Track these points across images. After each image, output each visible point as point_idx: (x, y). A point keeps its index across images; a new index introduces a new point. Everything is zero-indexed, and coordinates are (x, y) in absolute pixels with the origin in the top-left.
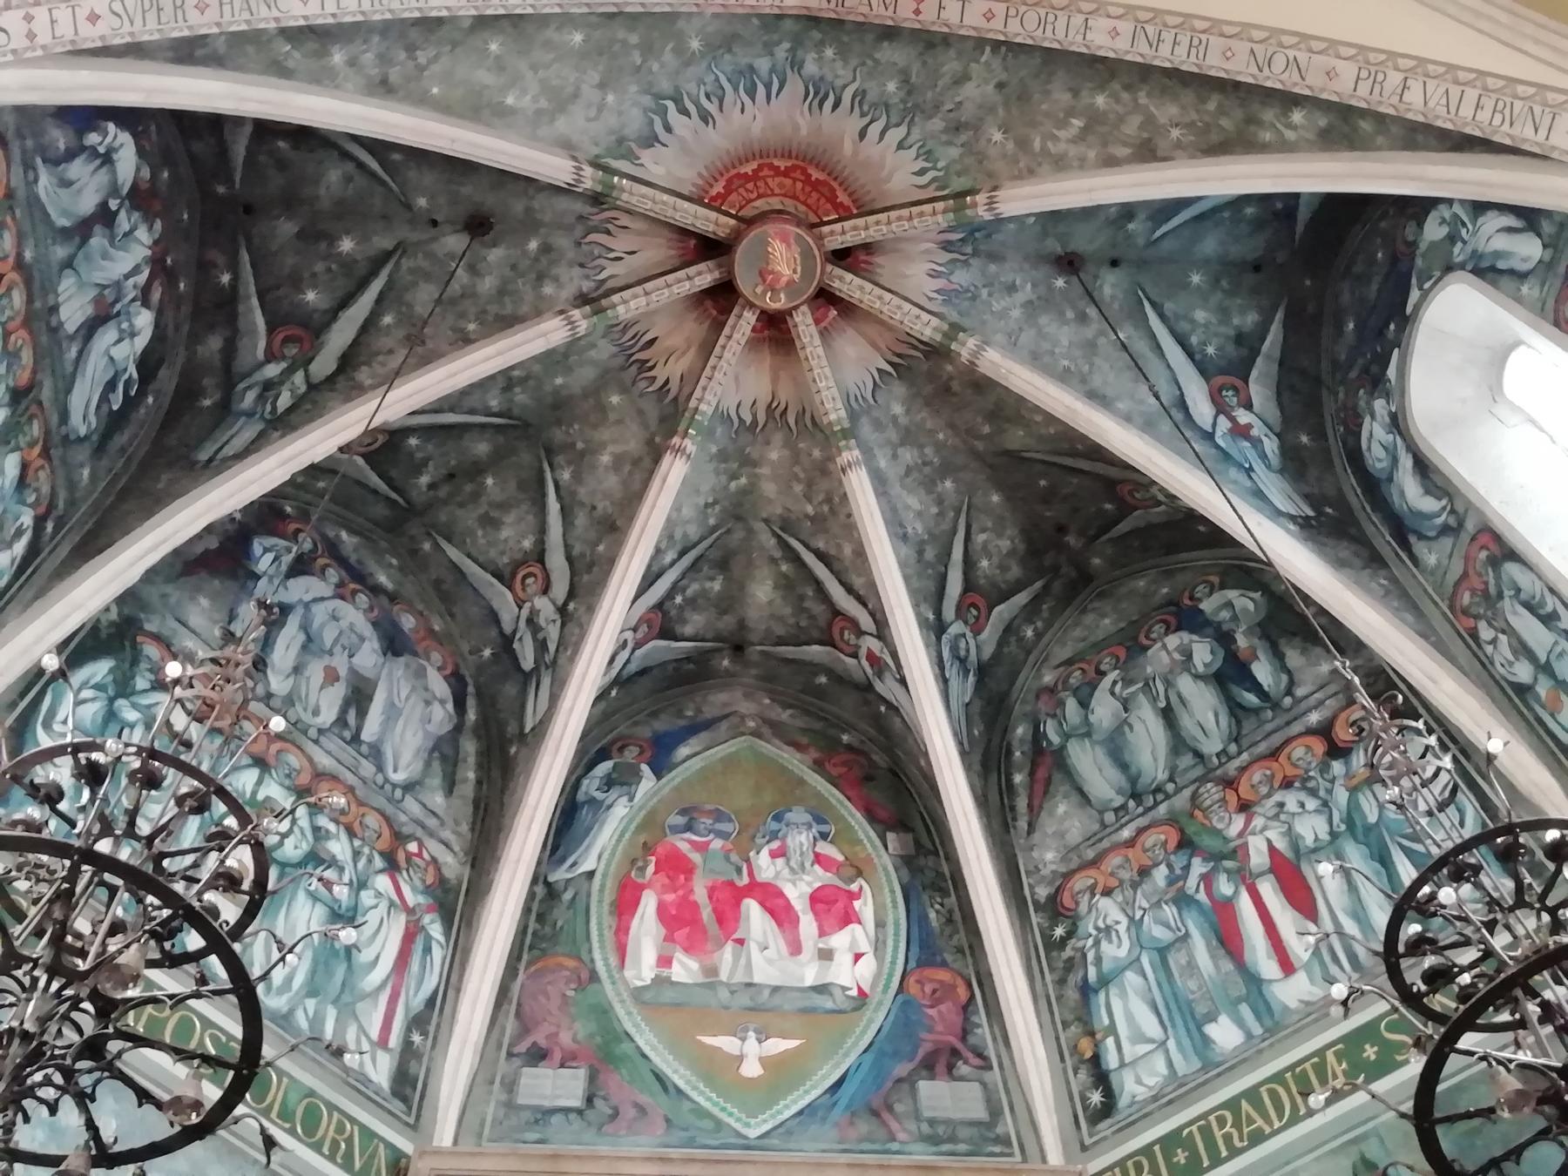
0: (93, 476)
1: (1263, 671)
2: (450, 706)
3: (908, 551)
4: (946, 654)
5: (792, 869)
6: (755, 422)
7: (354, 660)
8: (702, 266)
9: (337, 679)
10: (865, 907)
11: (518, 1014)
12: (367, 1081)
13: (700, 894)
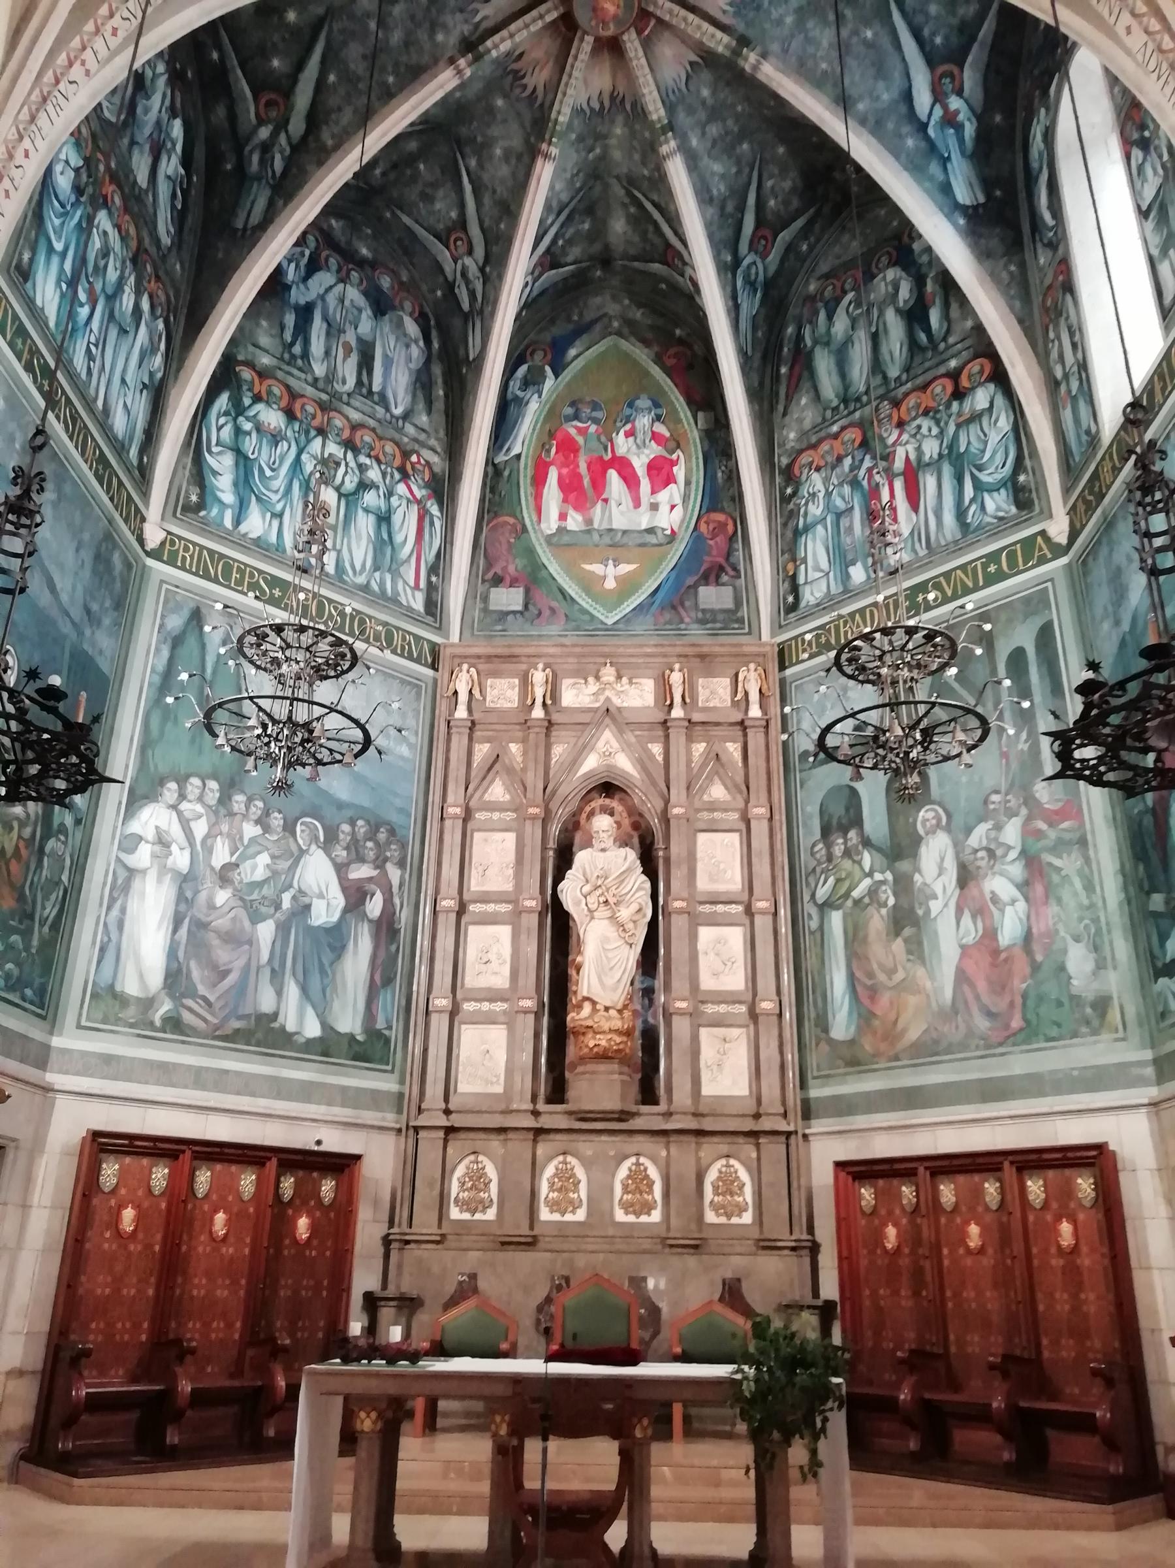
1: (935, 317)
2: (421, 343)
3: (711, 211)
4: (739, 283)
5: (638, 447)
7: (359, 330)
10: (679, 472)
12: (410, 609)
13: (583, 468)
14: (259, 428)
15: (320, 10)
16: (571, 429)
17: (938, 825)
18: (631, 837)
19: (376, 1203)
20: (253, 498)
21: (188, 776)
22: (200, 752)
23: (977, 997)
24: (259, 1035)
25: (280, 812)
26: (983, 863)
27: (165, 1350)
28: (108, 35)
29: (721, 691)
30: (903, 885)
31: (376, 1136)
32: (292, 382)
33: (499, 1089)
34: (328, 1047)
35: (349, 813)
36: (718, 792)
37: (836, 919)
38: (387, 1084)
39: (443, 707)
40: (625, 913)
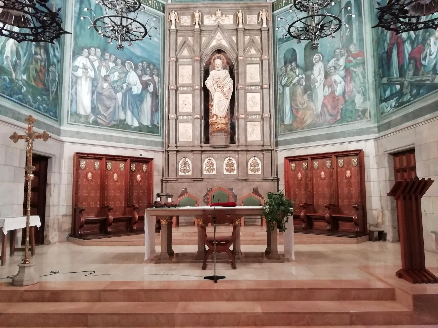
17: (320, 60)
18: (227, 67)
19: (158, 171)
21: (90, 48)
22: (93, 39)
23: (328, 111)
24: (121, 126)
26: (332, 71)
27: (104, 209)
29: (254, 19)
30: (308, 79)
31: (156, 153)
33: (191, 140)
34: (141, 129)
35: (141, 60)
36: (253, 52)
37: (287, 89)
39: (167, 25)
40: (225, 89)
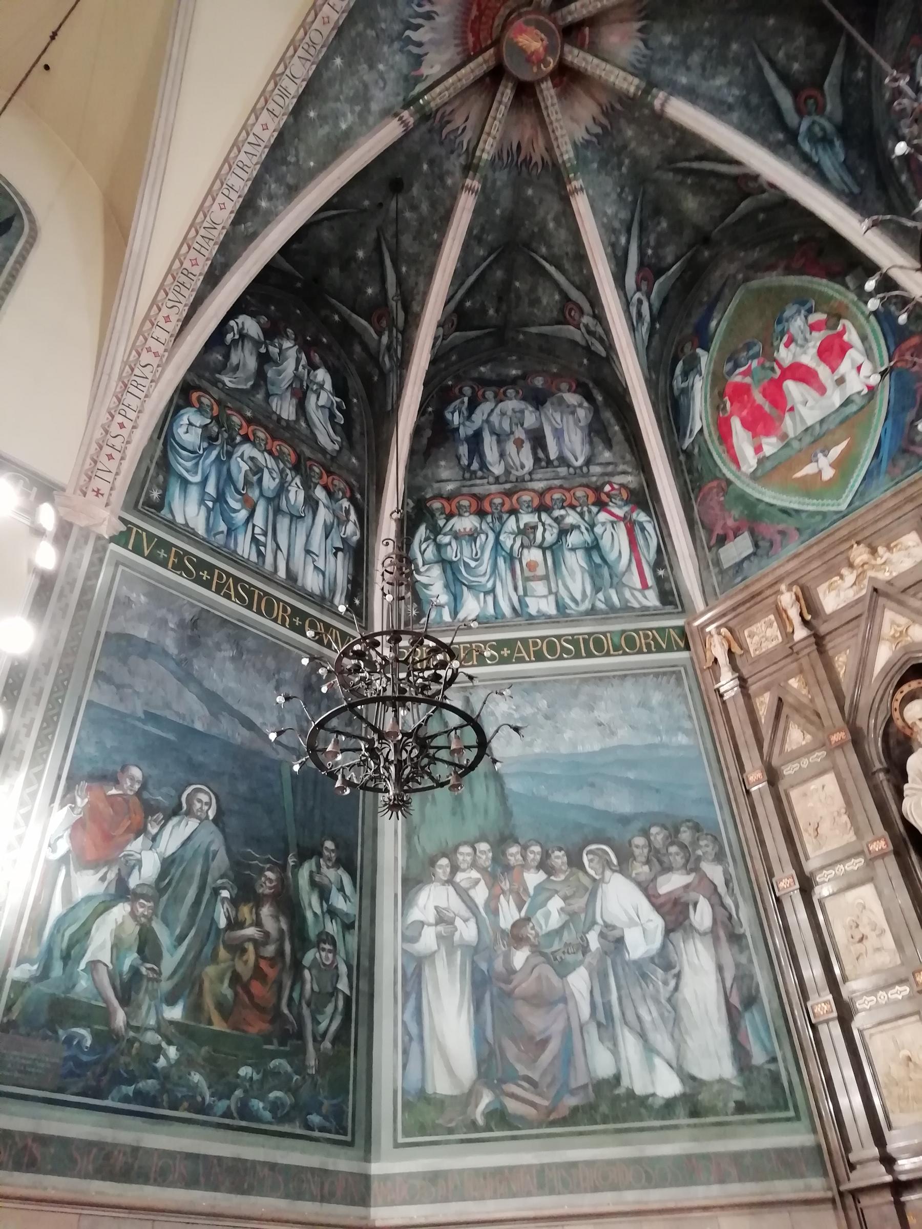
0: (358, 458)
2: (586, 404)
4: (806, 147)
5: (802, 346)
6: (603, 127)
7: (525, 426)
8: (501, 88)
9: (523, 442)
10: (852, 336)
11: (703, 527)
12: (645, 608)
13: (759, 398)
14: (457, 536)
15: (374, 235)
16: (737, 378)
20: (465, 588)
21: (456, 849)
24: (604, 1108)
25: (560, 849)
28: (162, 323)
32: (476, 490)
34: (693, 1104)
35: (637, 825)
38: (797, 1137)
